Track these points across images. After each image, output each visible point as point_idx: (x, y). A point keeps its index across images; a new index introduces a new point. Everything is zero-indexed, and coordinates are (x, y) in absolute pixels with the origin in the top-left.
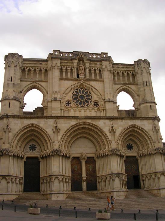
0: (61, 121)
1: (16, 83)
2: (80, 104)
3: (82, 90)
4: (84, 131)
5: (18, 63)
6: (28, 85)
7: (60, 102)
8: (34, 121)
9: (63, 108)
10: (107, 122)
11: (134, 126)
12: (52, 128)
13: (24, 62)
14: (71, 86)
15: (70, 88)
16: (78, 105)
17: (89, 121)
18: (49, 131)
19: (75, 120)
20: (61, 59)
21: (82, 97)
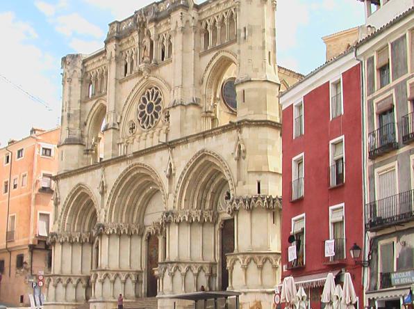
0: (109, 169)
1: (72, 112)
2: (147, 123)
3: (150, 92)
4: (146, 179)
5: (75, 71)
6: (94, 105)
7: (119, 130)
8: (81, 179)
9: (121, 142)
10: (165, 154)
11: (203, 154)
12: (98, 186)
13: (86, 65)
14: (133, 90)
15: (133, 95)
16: (143, 127)
17: (141, 160)
18: (95, 193)
19: (125, 162)
20: (118, 39)
21: (150, 106)
